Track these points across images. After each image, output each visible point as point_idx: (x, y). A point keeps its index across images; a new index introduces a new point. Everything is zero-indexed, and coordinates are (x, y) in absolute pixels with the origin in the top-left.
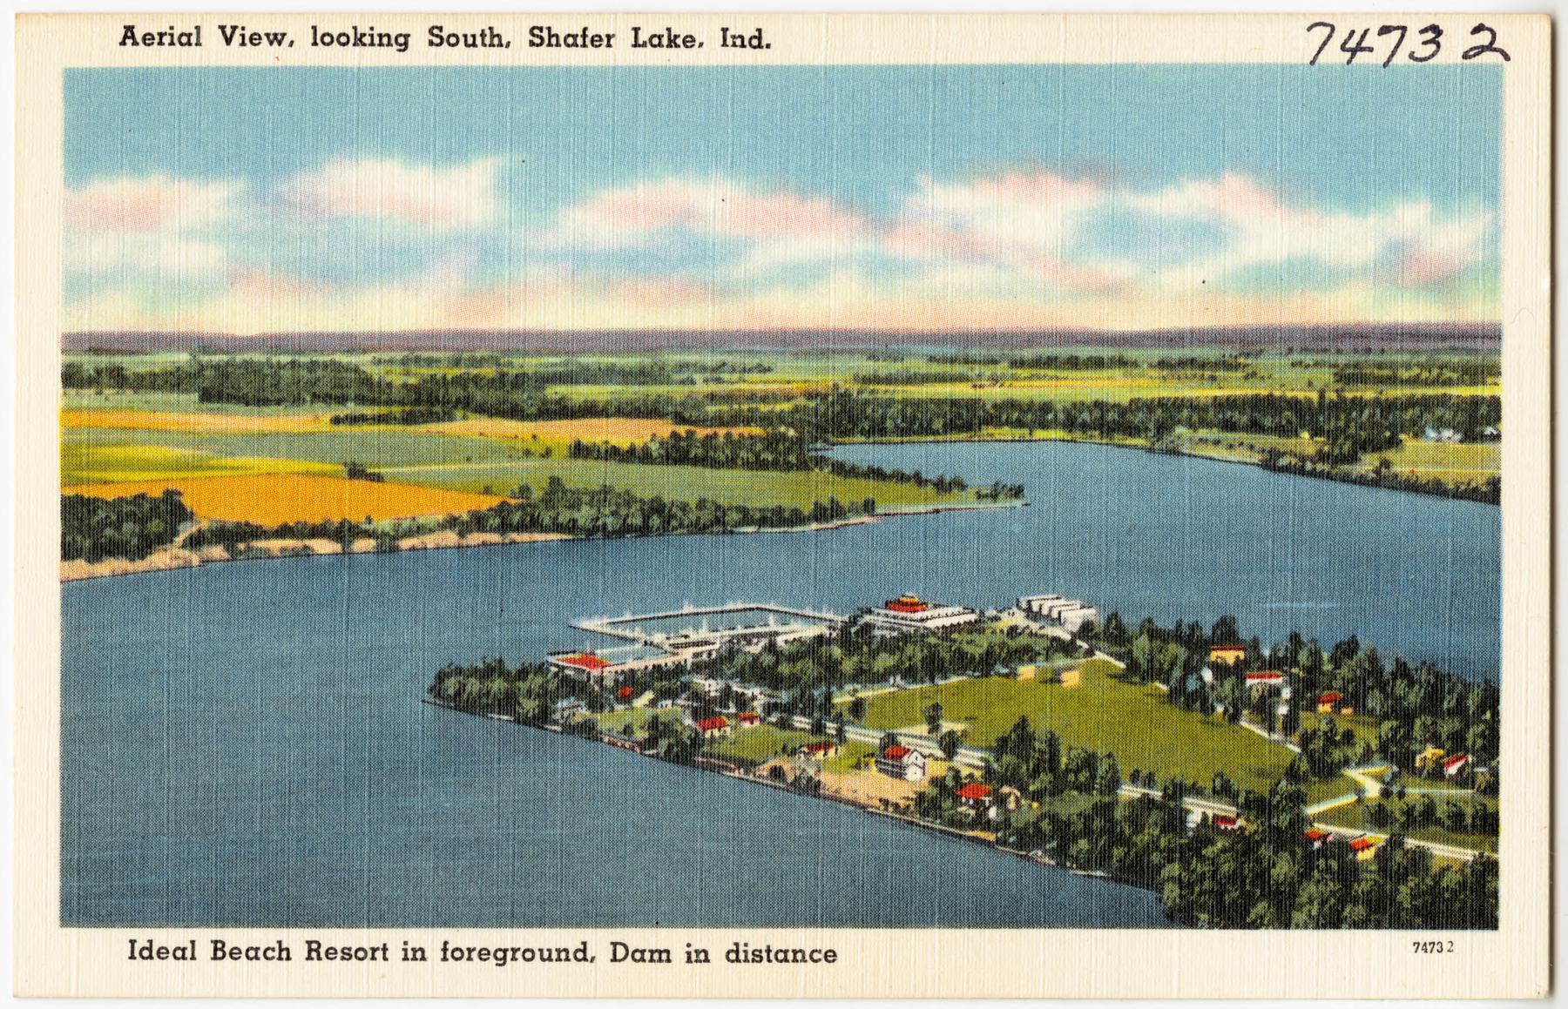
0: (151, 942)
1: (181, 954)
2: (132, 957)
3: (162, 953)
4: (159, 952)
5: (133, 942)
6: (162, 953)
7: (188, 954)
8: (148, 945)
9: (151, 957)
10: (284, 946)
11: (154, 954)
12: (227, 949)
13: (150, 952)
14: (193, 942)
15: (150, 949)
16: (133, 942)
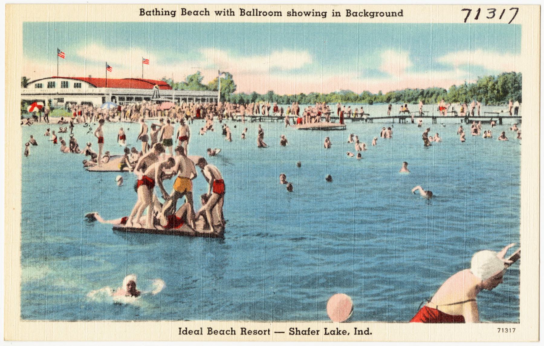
0: (186, 328)
1: (197, 332)
2: (180, 334)
3: (190, 332)
4: (189, 332)
5: (180, 329)
6: (190, 332)
7: (200, 332)
8: (185, 329)
9: (186, 334)
10: (233, 330)
11: (188, 333)
12: (213, 331)
13: (186, 332)
14: (201, 328)
15: (186, 331)
16: (180, 329)
